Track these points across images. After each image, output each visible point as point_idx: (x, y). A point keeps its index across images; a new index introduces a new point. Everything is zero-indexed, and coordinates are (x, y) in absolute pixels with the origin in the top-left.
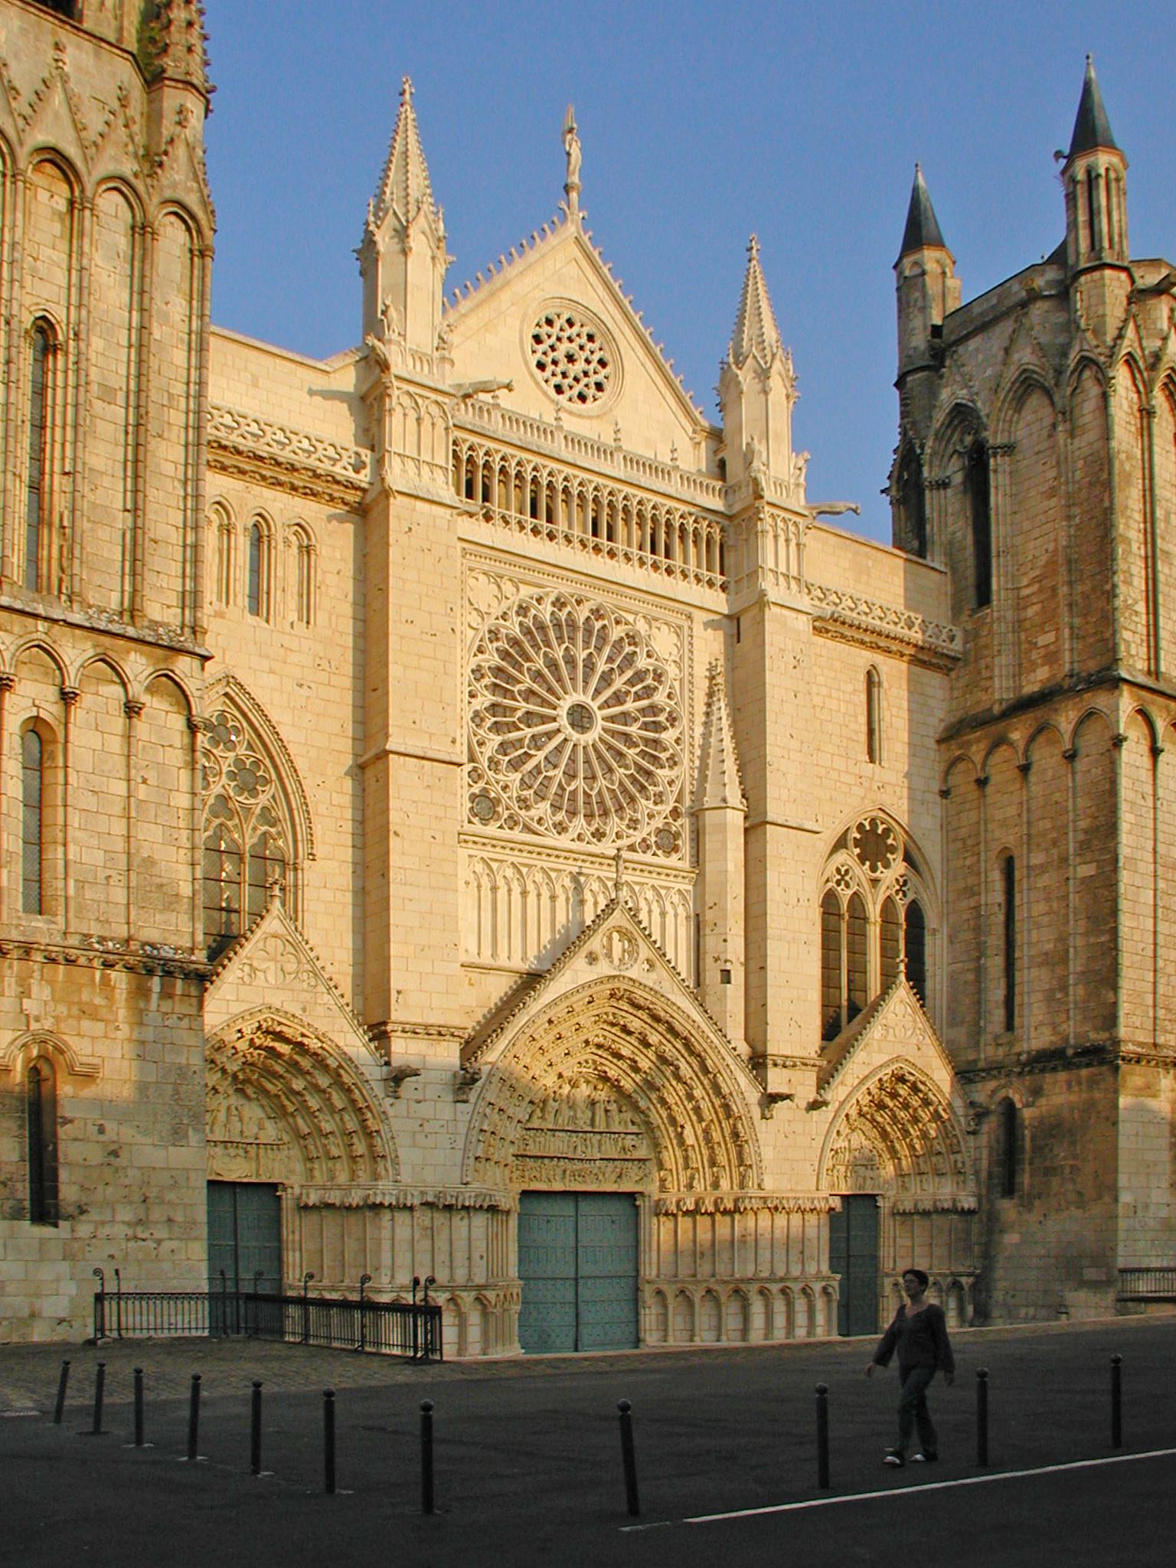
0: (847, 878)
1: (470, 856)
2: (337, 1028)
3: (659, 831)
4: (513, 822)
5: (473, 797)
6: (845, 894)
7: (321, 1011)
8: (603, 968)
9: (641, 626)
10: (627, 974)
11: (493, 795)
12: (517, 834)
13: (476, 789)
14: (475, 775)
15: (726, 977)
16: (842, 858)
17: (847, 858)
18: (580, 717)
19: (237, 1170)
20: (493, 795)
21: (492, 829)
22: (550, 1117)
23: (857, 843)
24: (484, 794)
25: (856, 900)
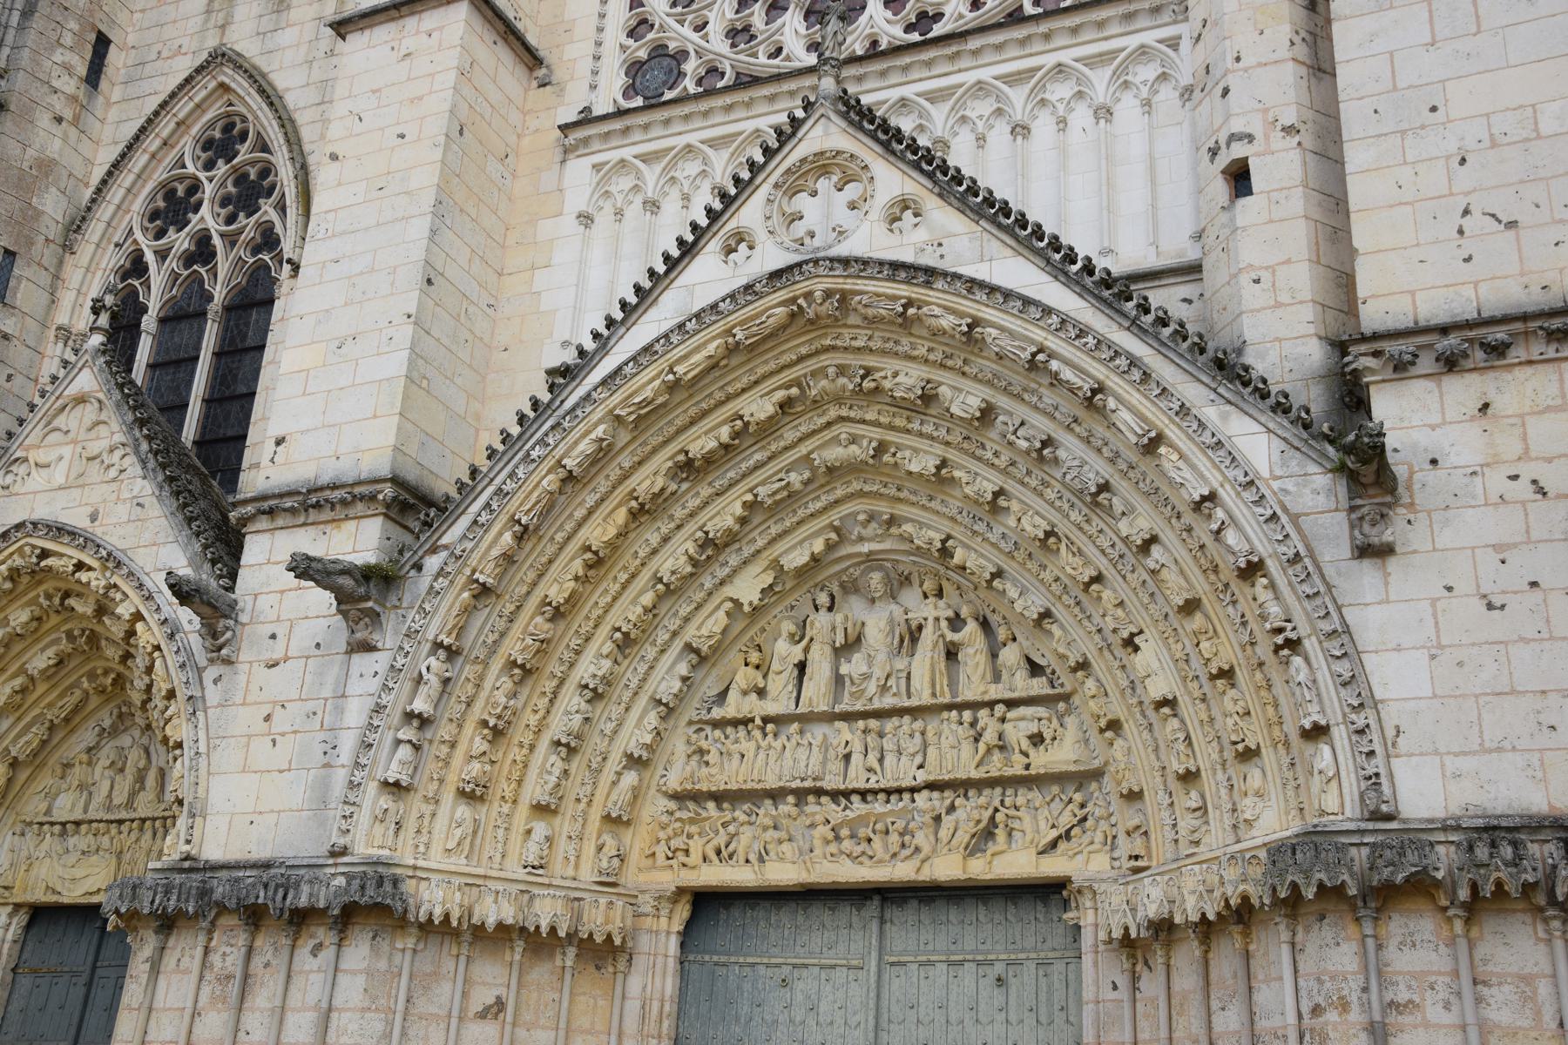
1: (597, 167)
2: (147, 537)
5: (635, 69)
7: (123, 511)
8: (770, 257)
10: (842, 250)
11: (672, 45)
15: (1239, 178)
20: (672, 45)
24: (659, 51)
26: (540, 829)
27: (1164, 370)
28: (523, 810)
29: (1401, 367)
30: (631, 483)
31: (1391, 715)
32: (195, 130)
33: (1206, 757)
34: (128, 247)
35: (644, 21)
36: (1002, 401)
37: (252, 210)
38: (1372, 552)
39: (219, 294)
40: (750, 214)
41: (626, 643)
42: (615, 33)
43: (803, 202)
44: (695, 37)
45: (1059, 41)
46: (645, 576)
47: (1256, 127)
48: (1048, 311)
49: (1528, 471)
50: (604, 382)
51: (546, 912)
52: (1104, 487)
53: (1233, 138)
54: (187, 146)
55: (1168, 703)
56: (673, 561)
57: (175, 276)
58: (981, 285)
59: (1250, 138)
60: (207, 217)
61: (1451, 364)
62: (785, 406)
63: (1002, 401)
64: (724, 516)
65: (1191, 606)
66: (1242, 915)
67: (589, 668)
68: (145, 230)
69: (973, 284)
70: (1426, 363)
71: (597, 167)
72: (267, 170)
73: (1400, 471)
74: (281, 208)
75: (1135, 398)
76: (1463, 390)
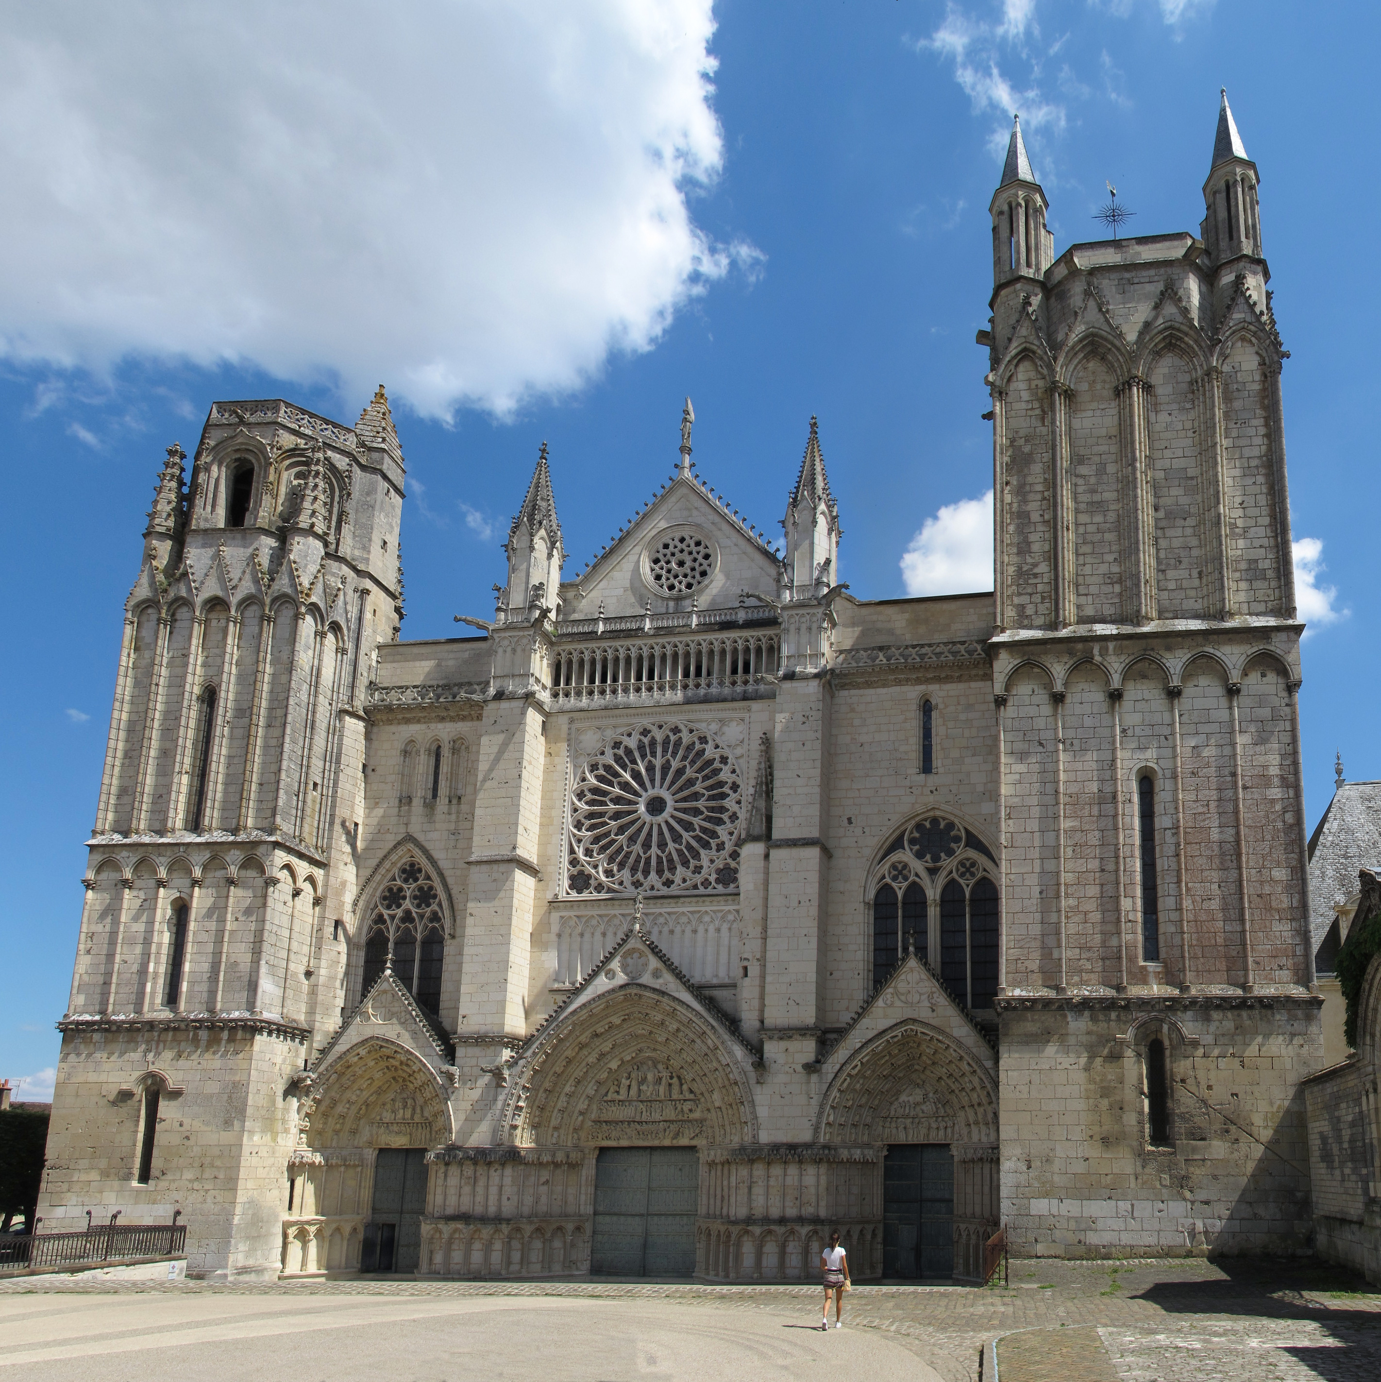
0: (905, 872)
1: (562, 917)
3: (719, 871)
4: (599, 888)
5: (572, 878)
6: (900, 889)
8: (621, 978)
9: (709, 728)
12: (603, 896)
13: (574, 871)
14: (574, 862)
16: (895, 857)
17: (906, 856)
18: (656, 806)
19: (399, 1141)
21: (585, 896)
22: (624, 1091)
23: (912, 842)
24: (581, 873)
25: (915, 891)
26: (556, 1134)
27: (721, 1030)
28: (551, 1130)
29: (771, 1038)
30: (580, 1039)
31: (760, 1120)
32: (399, 865)
33: (727, 1123)
34: (376, 911)
35: (575, 859)
36: (682, 1028)
37: (428, 905)
38: (758, 1082)
39: (419, 937)
40: (615, 965)
41: (579, 1082)
42: (565, 864)
43: (629, 960)
44: (593, 871)
45: (707, 903)
46: (584, 1063)
47: (750, 958)
48: (693, 1010)
49: (793, 1066)
50: (575, 1011)
51: (560, 1157)
52: (706, 1054)
53: (745, 959)
54: (396, 871)
55: (720, 1108)
56: (592, 1059)
57: (398, 928)
58: (677, 999)
59: (748, 960)
60: (407, 904)
61: (781, 1039)
62: (624, 1020)
63: (682, 1028)
64: (607, 1047)
65: (724, 1087)
66: (728, 1162)
67: (568, 1089)
68: (382, 904)
69: (675, 999)
70: (776, 1036)
71: (562, 917)
72: (431, 888)
73: (767, 1064)
74: (440, 905)
75: (712, 1037)
76: (783, 1044)
